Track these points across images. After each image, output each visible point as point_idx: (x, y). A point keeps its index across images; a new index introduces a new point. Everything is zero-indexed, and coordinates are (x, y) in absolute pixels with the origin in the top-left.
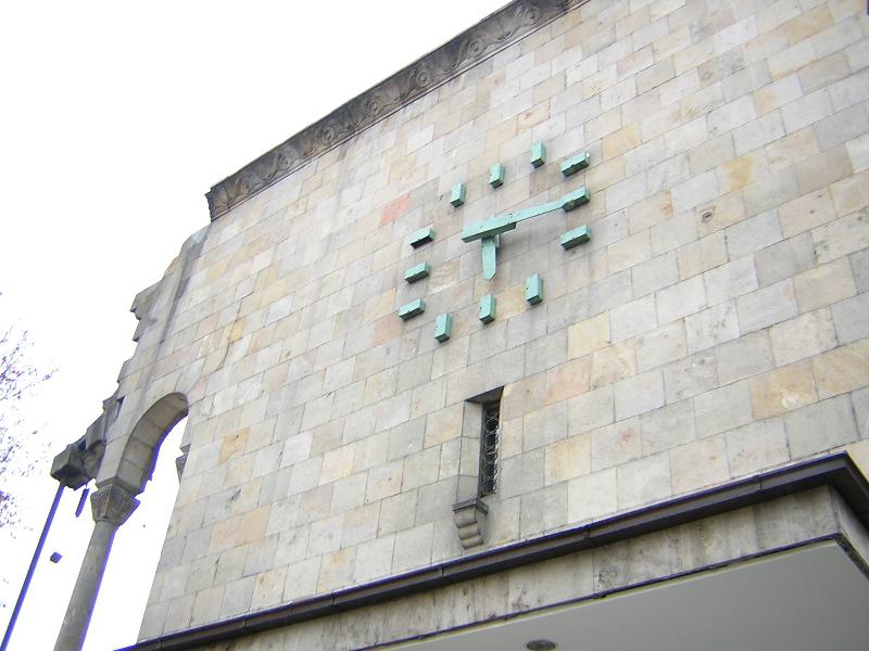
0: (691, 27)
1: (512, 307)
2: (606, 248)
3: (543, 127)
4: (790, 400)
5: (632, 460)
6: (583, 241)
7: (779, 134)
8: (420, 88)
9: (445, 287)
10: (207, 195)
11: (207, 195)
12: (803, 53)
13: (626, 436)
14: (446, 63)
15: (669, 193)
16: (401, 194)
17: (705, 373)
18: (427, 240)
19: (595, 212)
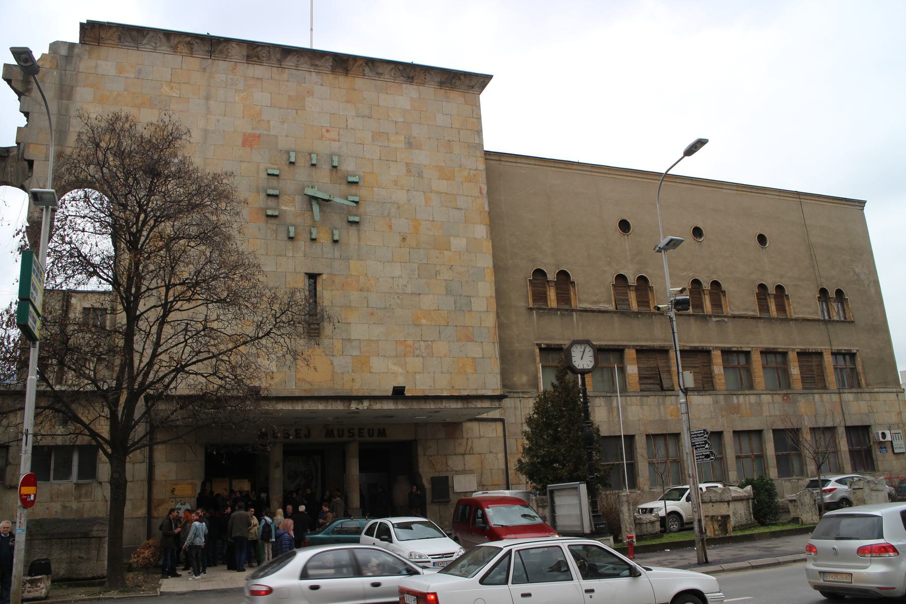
0: (405, 137)
1: (324, 238)
2: (366, 231)
3: (335, 145)
4: (424, 321)
5: (374, 323)
7: (431, 219)
8: (260, 59)
10: (82, 25)
11: (82, 25)
12: (442, 185)
13: (372, 314)
14: (279, 56)
15: (391, 220)
16: (254, 131)
17: (399, 302)
18: (277, 175)
19: (361, 210)
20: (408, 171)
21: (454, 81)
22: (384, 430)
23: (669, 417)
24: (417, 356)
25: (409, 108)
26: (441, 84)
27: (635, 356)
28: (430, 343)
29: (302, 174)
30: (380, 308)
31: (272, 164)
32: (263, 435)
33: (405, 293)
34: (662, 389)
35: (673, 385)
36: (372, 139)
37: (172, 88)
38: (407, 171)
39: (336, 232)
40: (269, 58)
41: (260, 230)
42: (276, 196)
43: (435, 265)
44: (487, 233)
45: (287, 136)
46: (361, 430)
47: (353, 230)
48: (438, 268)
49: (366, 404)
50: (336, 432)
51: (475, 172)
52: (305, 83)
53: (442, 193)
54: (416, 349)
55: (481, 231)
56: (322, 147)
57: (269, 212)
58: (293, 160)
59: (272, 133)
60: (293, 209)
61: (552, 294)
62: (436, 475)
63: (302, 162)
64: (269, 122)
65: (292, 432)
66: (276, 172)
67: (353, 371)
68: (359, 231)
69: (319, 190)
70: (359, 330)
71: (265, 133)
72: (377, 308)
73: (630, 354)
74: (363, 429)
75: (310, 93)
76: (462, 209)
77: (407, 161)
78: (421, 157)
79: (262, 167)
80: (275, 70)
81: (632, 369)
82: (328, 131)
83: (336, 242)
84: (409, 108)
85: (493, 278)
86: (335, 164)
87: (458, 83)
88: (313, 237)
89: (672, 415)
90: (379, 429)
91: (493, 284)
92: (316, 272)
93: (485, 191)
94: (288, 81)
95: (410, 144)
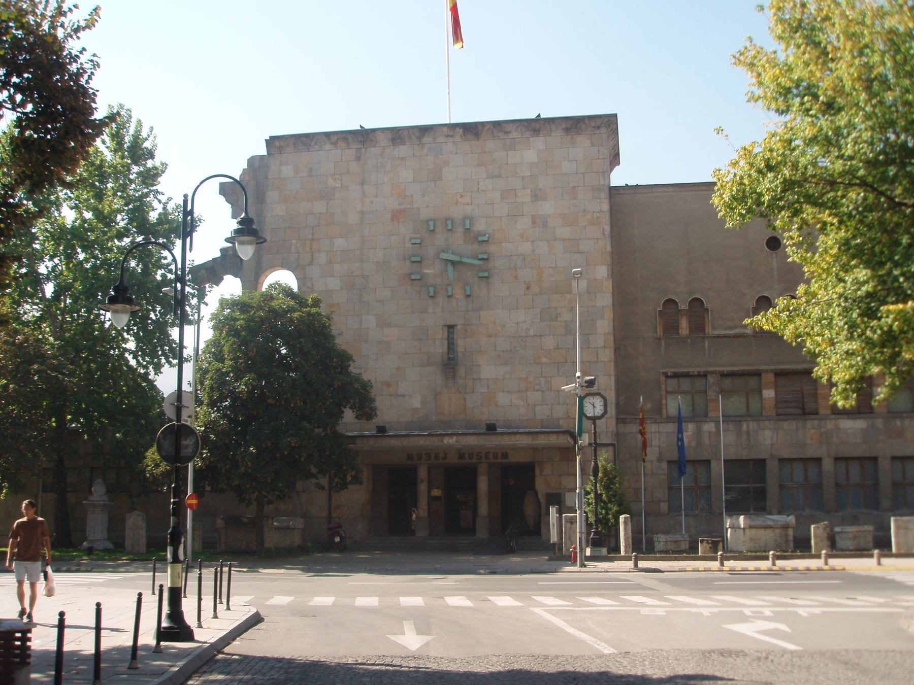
0: (532, 191)
1: (459, 295)
3: (469, 208)
4: (544, 360)
5: (500, 364)
6: (486, 277)
9: (429, 271)
13: (499, 356)
14: (418, 134)
15: (516, 270)
20: (534, 223)
21: (579, 125)
22: (506, 453)
23: (809, 441)
24: (537, 390)
25: (536, 160)
26: (567, 130)
27: (773, 380)
28: (549, 379)
29: (440, 240)
30: (507, 351)
31: (416, 234)
32: (410, 457)
33: (528, 336)
34: (804, 414)
35: (817, 409)
36: (502, 198)
37: (335, 180)
38: (532, 223)
39: (468, 288)
40: (410, 138)
41: (406, 292)
42: (420, 262)
43: (556, 308)
44: (608, 273)
45: (427, 207)
46: (487, 454)
48: (558, 312)
49: (455, 438)
50: (467, 455)
51: (598, 215)
52: (442, 155)
53: (565, 240)
54: (537, 385)
55: (602, 272)
56: (457, 212)
57: (413, 277)
58: (432, 228)
59: (415, 206)
60: (432, 271)
61: (684, 325)
62: (551, 491)
64: (412, 196)
65: (433, 457)
66: (418, 241)
67: (482, 406)
69: (453, 253)
70: (488, 371)
71: (409, 206)
72: (503, 351)
73: (771, 377)
74: (489, 453)
75: (447, 163)
76: (584, 252)
77: (534, 214)
78: (547, 208)
79: (407, 238)
80: (416, 147)
81: (769, 394)
82: (462, 196)
83: (468, 296)
84: (536, 160)
85: (612, 315)
86: (468, 227)
87: (583, 126)
88: (450, 294)
89: (812, 439)
90: (503, 453)
91: (611, 321)
92: (452, 323)
93: (608, 232)
94: (427, 155)
95: (537, 196)
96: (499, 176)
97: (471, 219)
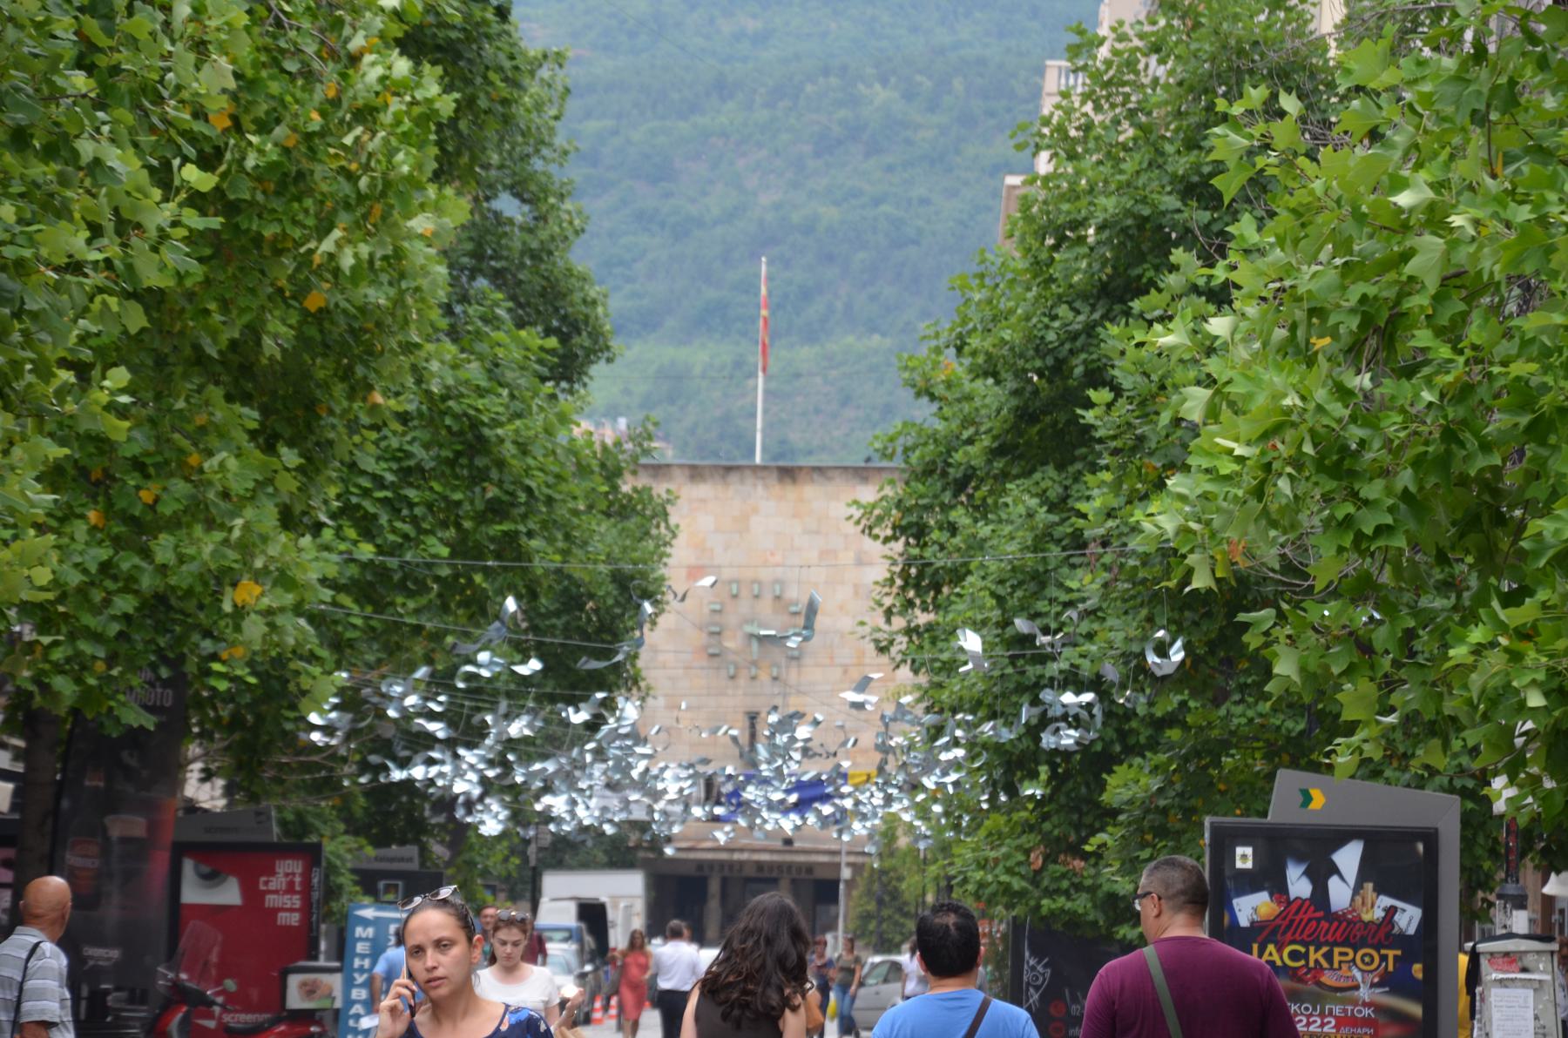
1: (764, 677)
3: (779, 570)
20: (856, 593)
29: (744, 606)
47: (794, 663)
56: (765, 574)
57: (711, 651)
63: (745, 593)
68: (799, 666)
75: (755, 511)
96: (817, 532)
97: (780, 582)
